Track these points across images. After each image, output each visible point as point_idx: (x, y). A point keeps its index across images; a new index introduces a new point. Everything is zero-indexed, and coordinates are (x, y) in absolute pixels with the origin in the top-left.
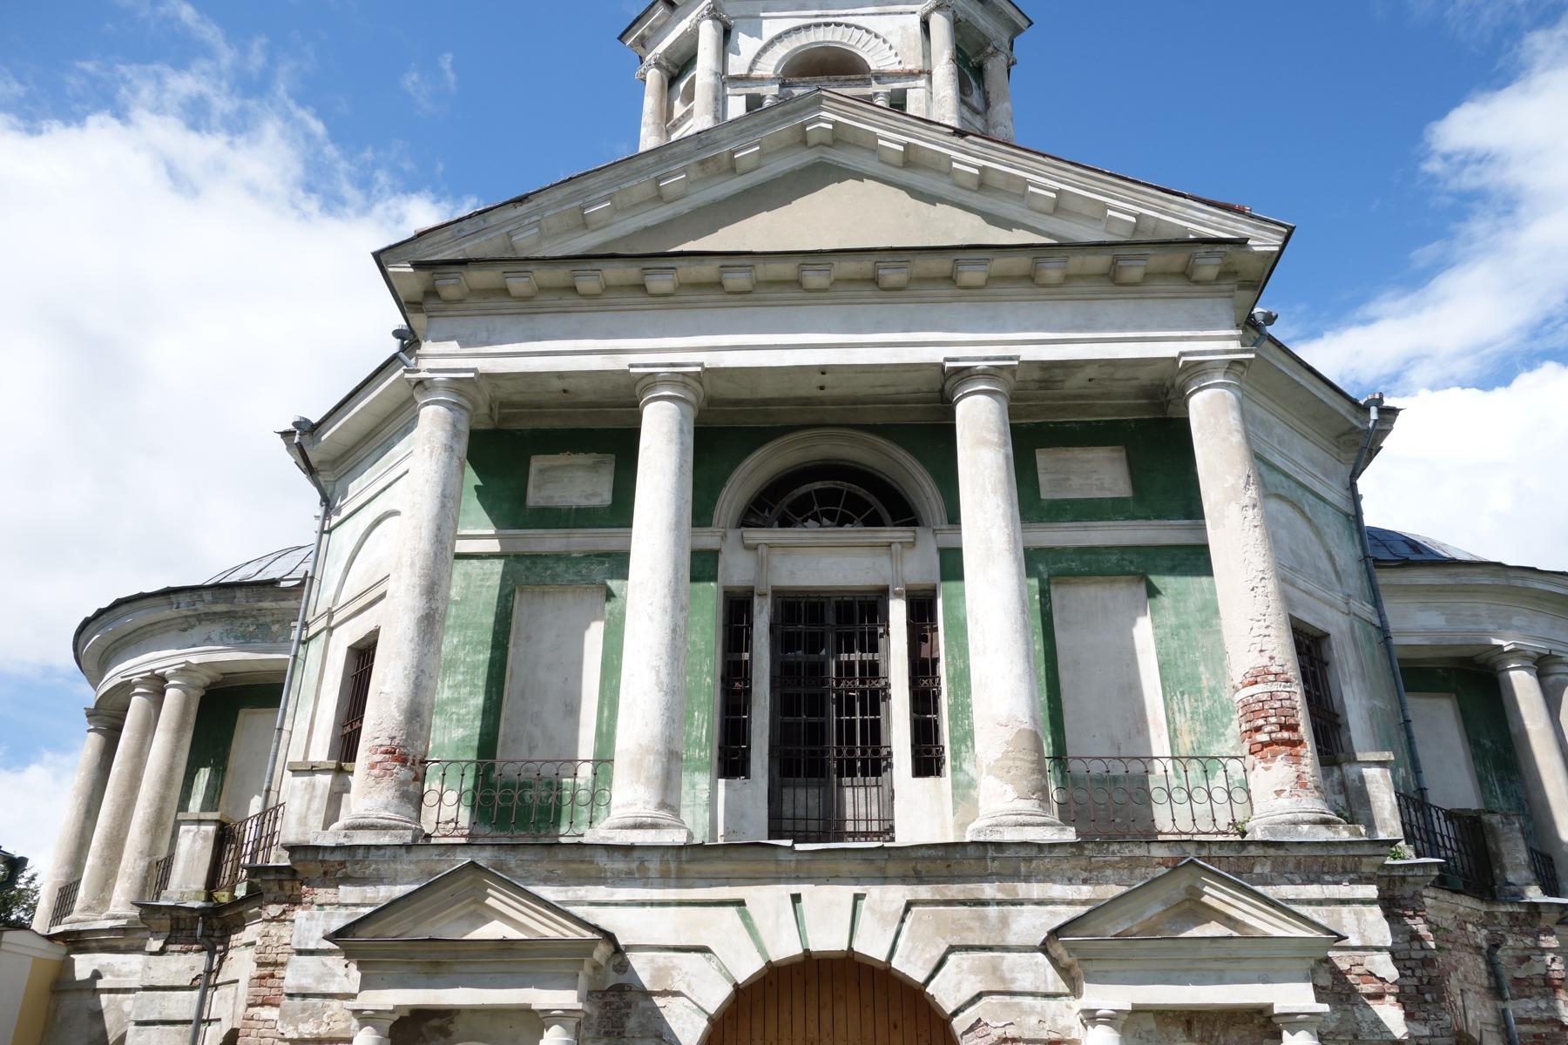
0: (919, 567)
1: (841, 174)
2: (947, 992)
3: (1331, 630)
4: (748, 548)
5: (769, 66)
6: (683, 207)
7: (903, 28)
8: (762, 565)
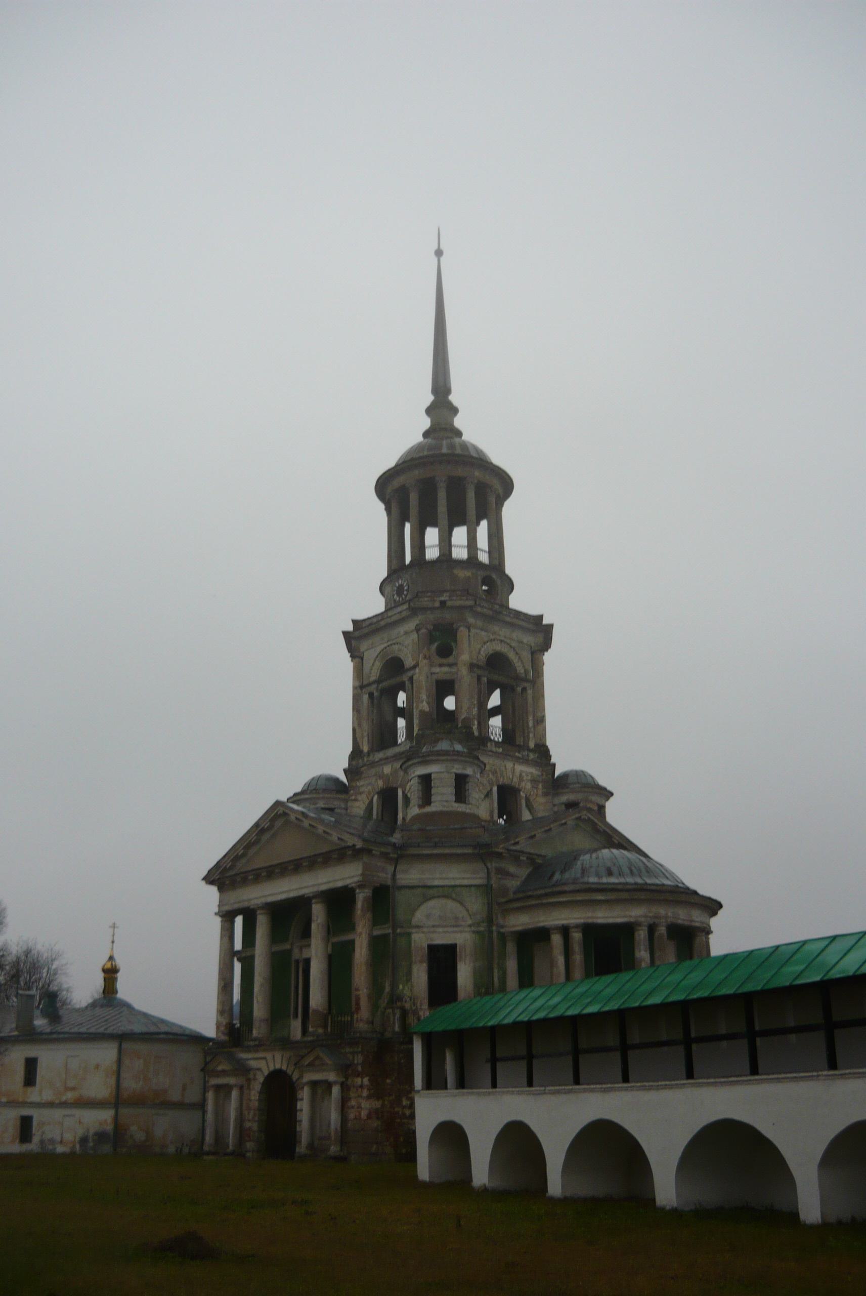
5: (374, 675)
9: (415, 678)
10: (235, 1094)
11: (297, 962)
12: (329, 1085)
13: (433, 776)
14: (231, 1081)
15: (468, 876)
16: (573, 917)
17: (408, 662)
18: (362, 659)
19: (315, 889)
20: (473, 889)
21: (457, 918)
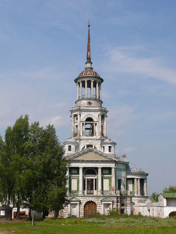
0: (96, 177)
1: (91, 151)
10: (78, 205)
12: (110, 204)
14: (78, 203)
17: (95, 120)
18: (80, 115)
19: (100, 166)
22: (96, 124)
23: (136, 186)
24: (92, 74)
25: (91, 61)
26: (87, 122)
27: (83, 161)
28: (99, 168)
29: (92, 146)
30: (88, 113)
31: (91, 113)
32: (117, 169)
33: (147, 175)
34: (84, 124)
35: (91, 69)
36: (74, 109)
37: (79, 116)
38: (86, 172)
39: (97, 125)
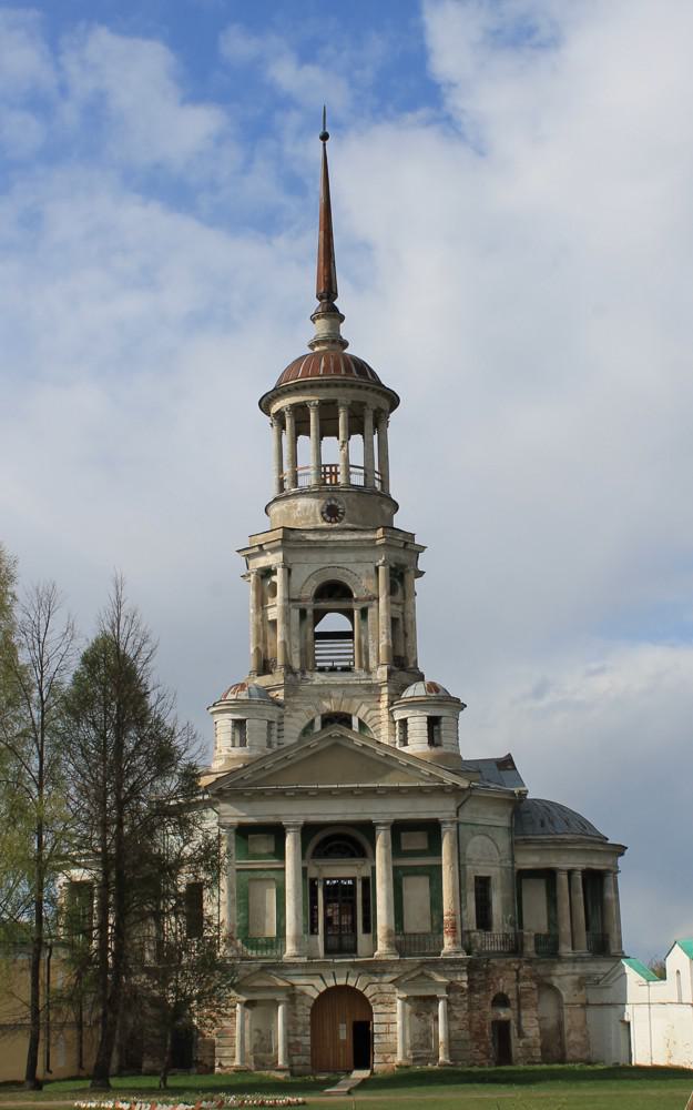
0: (366, 872)
2: (368, 993)
3: (492, 875)
4: (317, 866)
6: (293, 761)
7: (367, 571)
8: (320, 870)
9: (369, 611)
11: (313, 881)
13: (443, 720)
15: (497, 817)
16: (579, 863)
20: (500, 829)
21: (490, 854)
22: (364, 613)
23: (564, 906)
24: (343, 372)
25: (335, 309)
26: (323, 605)
27: (303, 794)
28: (378, 824)
29: (344, 719)
30: (328, 558)
31: (339, 558)
32: (469, 826)
33: (620, 850)
34: (309, 612)
35: (337, 346)
36: (260, 540)
37: (278, 579)
38: (317, 847)
39: (369, 617)
